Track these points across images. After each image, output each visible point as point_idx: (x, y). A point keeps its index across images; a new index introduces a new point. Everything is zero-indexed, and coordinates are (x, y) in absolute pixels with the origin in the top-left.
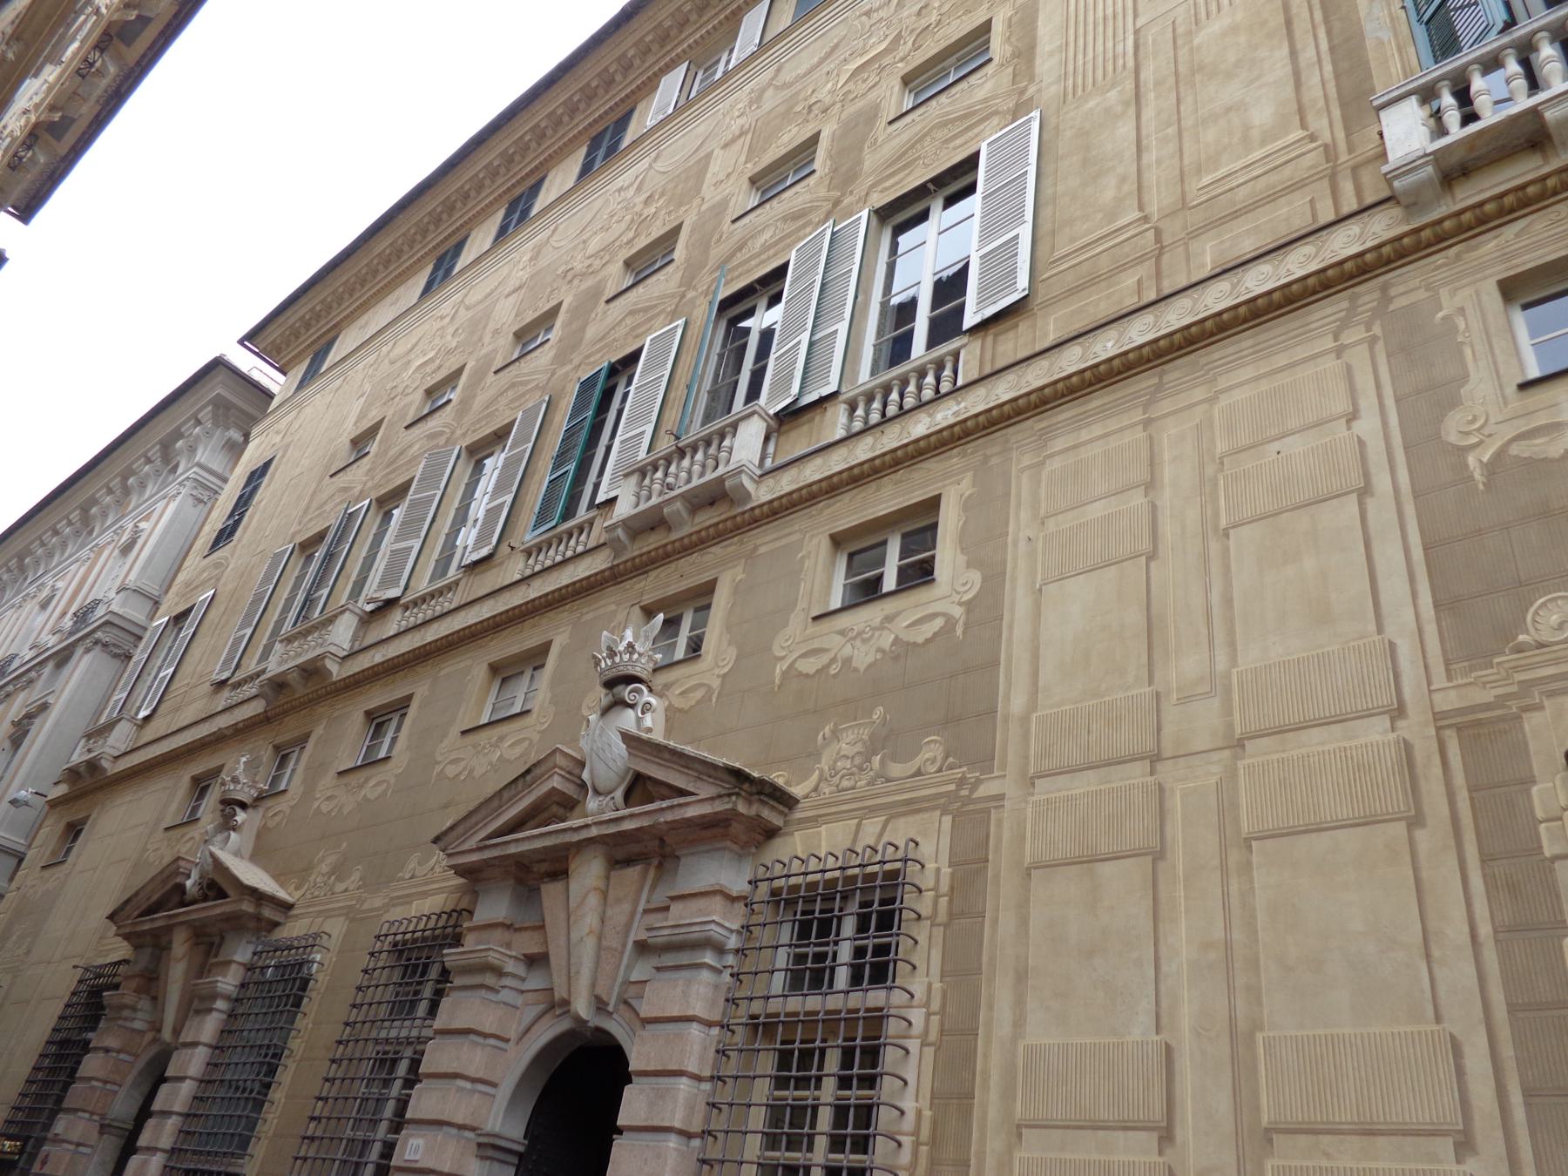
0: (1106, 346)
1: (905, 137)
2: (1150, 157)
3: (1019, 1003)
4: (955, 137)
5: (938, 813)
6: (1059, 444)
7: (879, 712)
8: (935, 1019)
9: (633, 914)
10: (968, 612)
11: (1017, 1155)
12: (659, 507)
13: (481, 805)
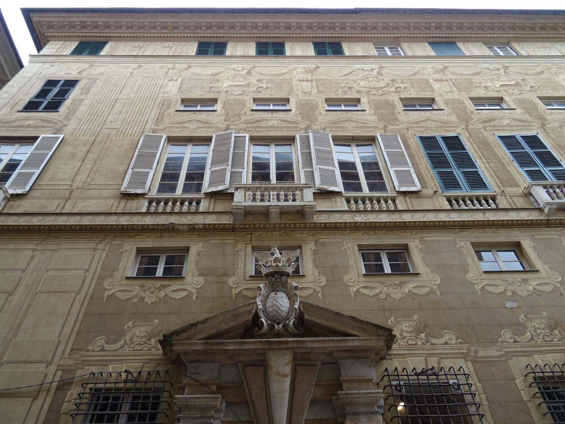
7: (416, 317)
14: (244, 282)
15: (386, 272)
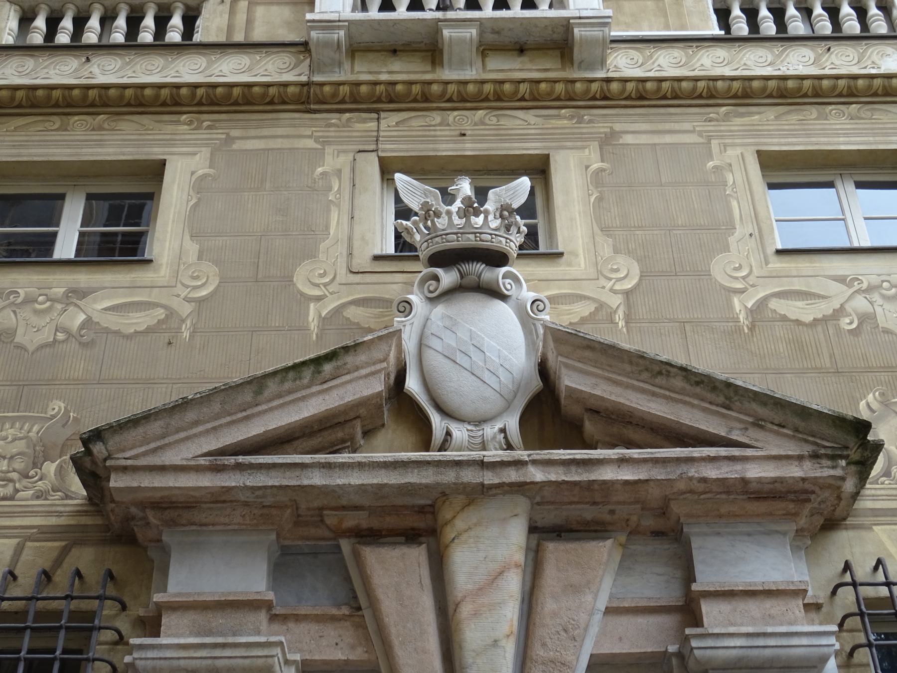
13: (216, 391)
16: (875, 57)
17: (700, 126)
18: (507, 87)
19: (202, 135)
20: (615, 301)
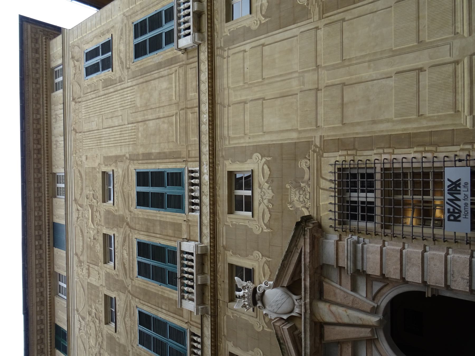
0: (205, 128)
1: (120, 199)
2: (161, 115)
3: (381, 122)
4: (128, 180)
5: (322, 159)
6: (226, 133)
7: (288, 186)
8: (386, 151)
9: (340, 289)
10: (264, 156)
11: (428, 115)
12: (198, 285)
14: (258, 317)
15: (251, 194)
16: (205, 181)
17: (221, 226)
18: (212, 269)
19: (223, 341)
20: (264, 259)
